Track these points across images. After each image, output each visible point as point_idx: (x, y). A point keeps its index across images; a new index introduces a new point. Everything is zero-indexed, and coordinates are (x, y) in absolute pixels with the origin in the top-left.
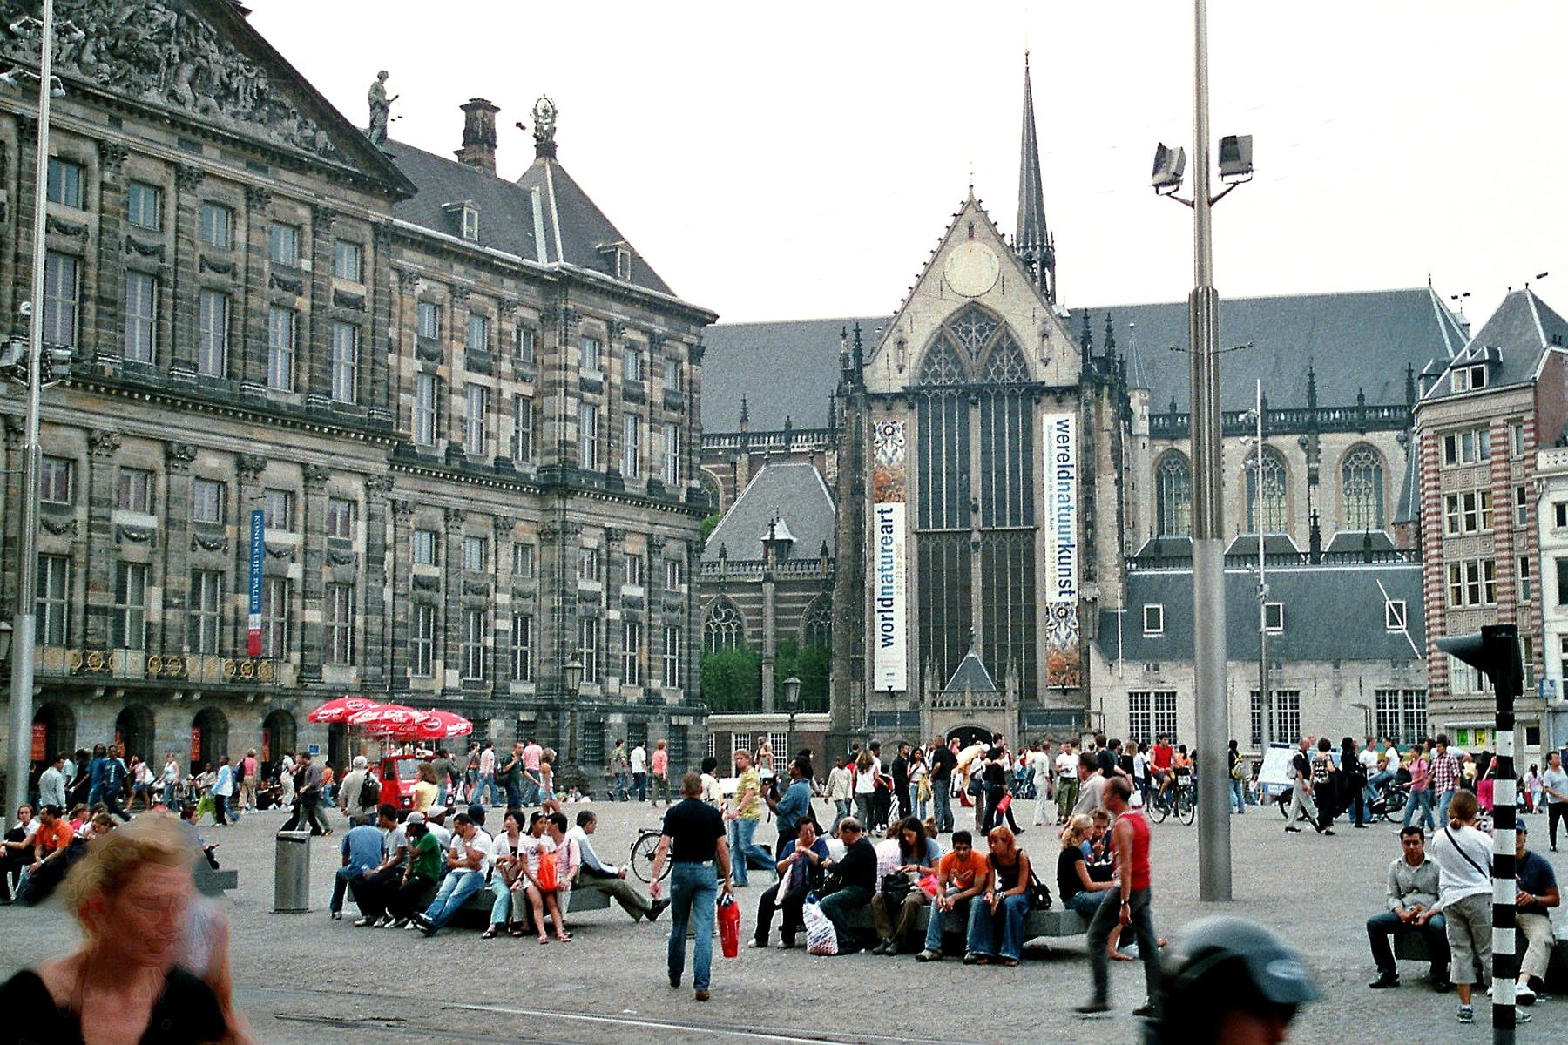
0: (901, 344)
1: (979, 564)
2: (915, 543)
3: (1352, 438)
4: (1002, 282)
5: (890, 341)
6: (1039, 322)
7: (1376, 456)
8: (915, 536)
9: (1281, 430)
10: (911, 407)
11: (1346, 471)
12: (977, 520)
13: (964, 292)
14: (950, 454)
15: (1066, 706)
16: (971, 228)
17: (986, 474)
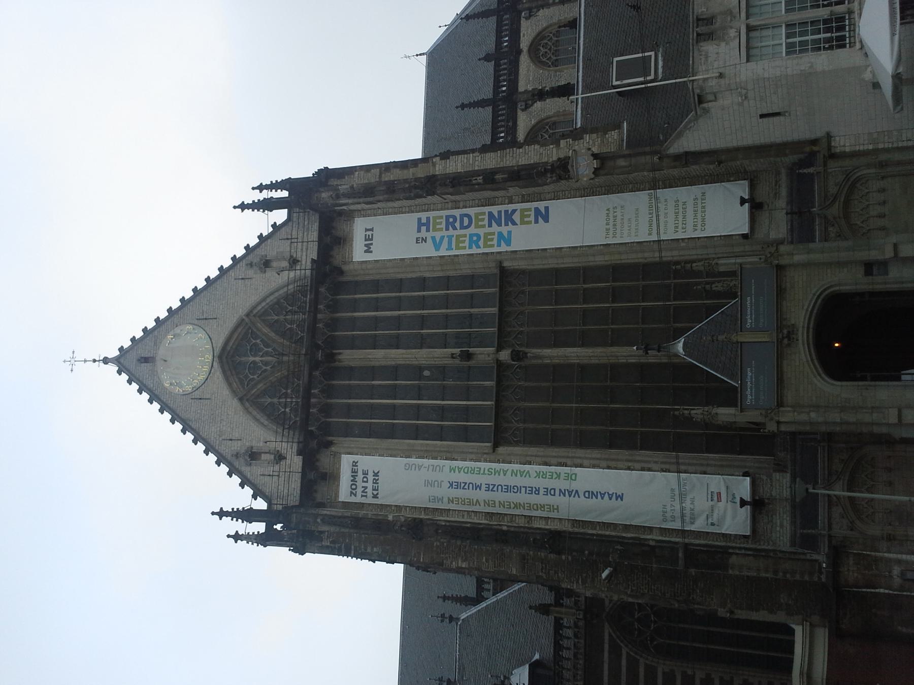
0: (253, 456)
1: (547, 352)
2: (510, 449)
3: (525, 61)
4: (203, 321)
5: (246, 470)
6: (251, 273)
7: (544, 38)
8: (501, 450)
9: (512, 130)
10: (330, 444)
11: (555, 64)
12: (484, 354)
13: (206, 369)
14: (393, 392)
15: (782, 203)
16: (146, 360)
17: (422, 343)
